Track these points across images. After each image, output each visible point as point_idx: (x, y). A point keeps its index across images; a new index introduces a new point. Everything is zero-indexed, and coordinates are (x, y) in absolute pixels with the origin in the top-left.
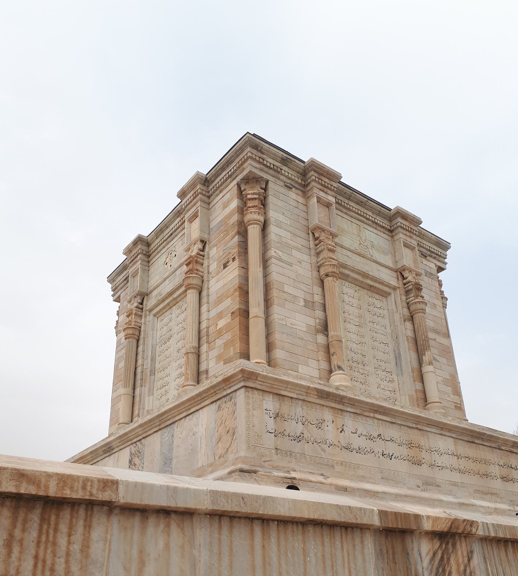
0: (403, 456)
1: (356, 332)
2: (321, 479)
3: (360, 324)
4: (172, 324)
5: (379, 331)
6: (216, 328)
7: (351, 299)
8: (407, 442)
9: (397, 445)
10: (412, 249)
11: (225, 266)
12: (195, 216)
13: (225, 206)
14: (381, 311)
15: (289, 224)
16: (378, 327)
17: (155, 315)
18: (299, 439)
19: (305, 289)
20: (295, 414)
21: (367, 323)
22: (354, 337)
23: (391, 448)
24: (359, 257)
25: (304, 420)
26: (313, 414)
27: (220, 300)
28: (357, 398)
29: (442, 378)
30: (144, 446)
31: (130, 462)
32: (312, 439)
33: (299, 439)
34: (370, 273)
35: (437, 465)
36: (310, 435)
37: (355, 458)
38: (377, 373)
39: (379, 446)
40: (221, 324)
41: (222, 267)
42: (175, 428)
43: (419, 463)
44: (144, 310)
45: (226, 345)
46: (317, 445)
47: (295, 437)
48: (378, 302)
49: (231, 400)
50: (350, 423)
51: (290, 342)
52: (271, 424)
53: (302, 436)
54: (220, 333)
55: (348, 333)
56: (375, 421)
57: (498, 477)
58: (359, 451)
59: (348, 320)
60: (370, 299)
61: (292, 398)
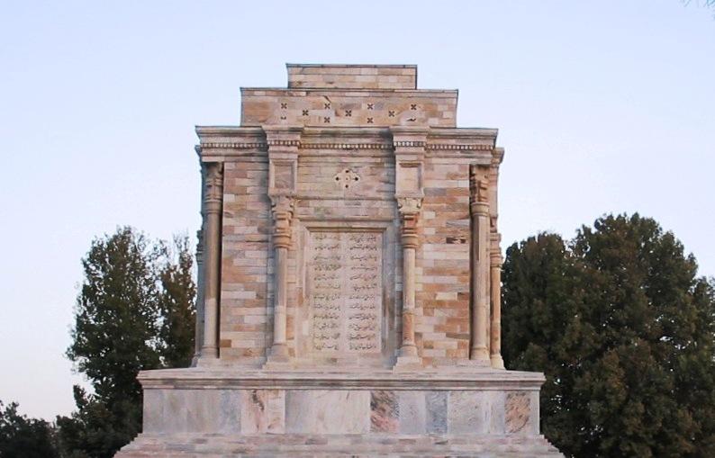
4: (340, 252)
6: (435, 297)
11: (450, 241)
12: (411, 165)
13: (453, 176)
17: (308, 228)
27: (436, 271)
30: (398, 397)
31: (374, 406)
40: (441, 296)
41: (445, 239)
42: (449, 395)
44: (295, 216)
45: (450, 320)
49: (524, 394)
54: (441, 304)
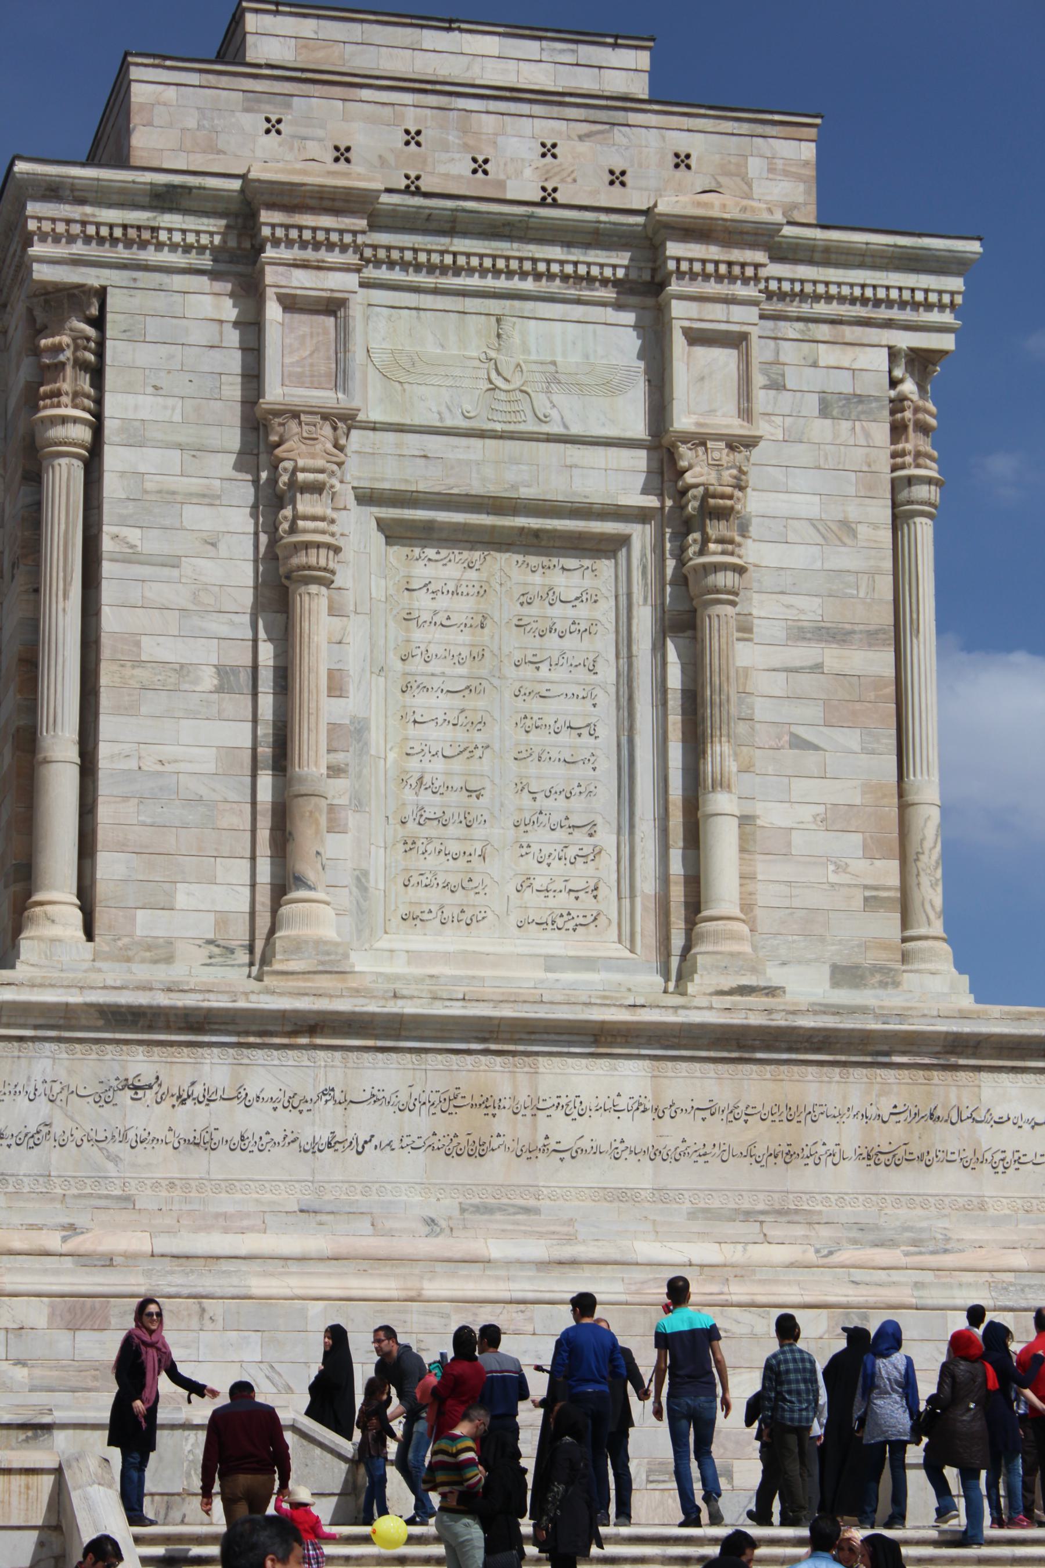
0: (414, 1137)
1: (452, 717)
2: (53, 1241)
3: (474, 683)
5: (556, 690)
7: (443, 602)
8: (434, 1098)
9: (391, 1109)
10: (736, 340)
14: (583, 611)
15: (177, 418)
16: (560, 674)
18: (32, 1140)
19: (225, 631)
20: (29, 1079)
21: (510, 671)
22: (439, 736)
24: (476, 443)
25: (57, 1088)
28: (242, 1004)
29: (821, 809)
32: (78, 1135)
33: (32, 1140)
34: (525, 492)
35: (553, 1146)
36: (71, 1124)
37: (223, 1163)
38: (525, 839)
43: (479, 1150)
46: (95, 1148)
47: (22, 1136)
48: (570, 577)
51: (149, 821)
53: (43, 1133)
55: (412, 731)
56: (321, 1054)
57: (849, 1153)
58: (241, 1144)
59: (420, 679)
60: (537, 579)
61: (21, 1039)
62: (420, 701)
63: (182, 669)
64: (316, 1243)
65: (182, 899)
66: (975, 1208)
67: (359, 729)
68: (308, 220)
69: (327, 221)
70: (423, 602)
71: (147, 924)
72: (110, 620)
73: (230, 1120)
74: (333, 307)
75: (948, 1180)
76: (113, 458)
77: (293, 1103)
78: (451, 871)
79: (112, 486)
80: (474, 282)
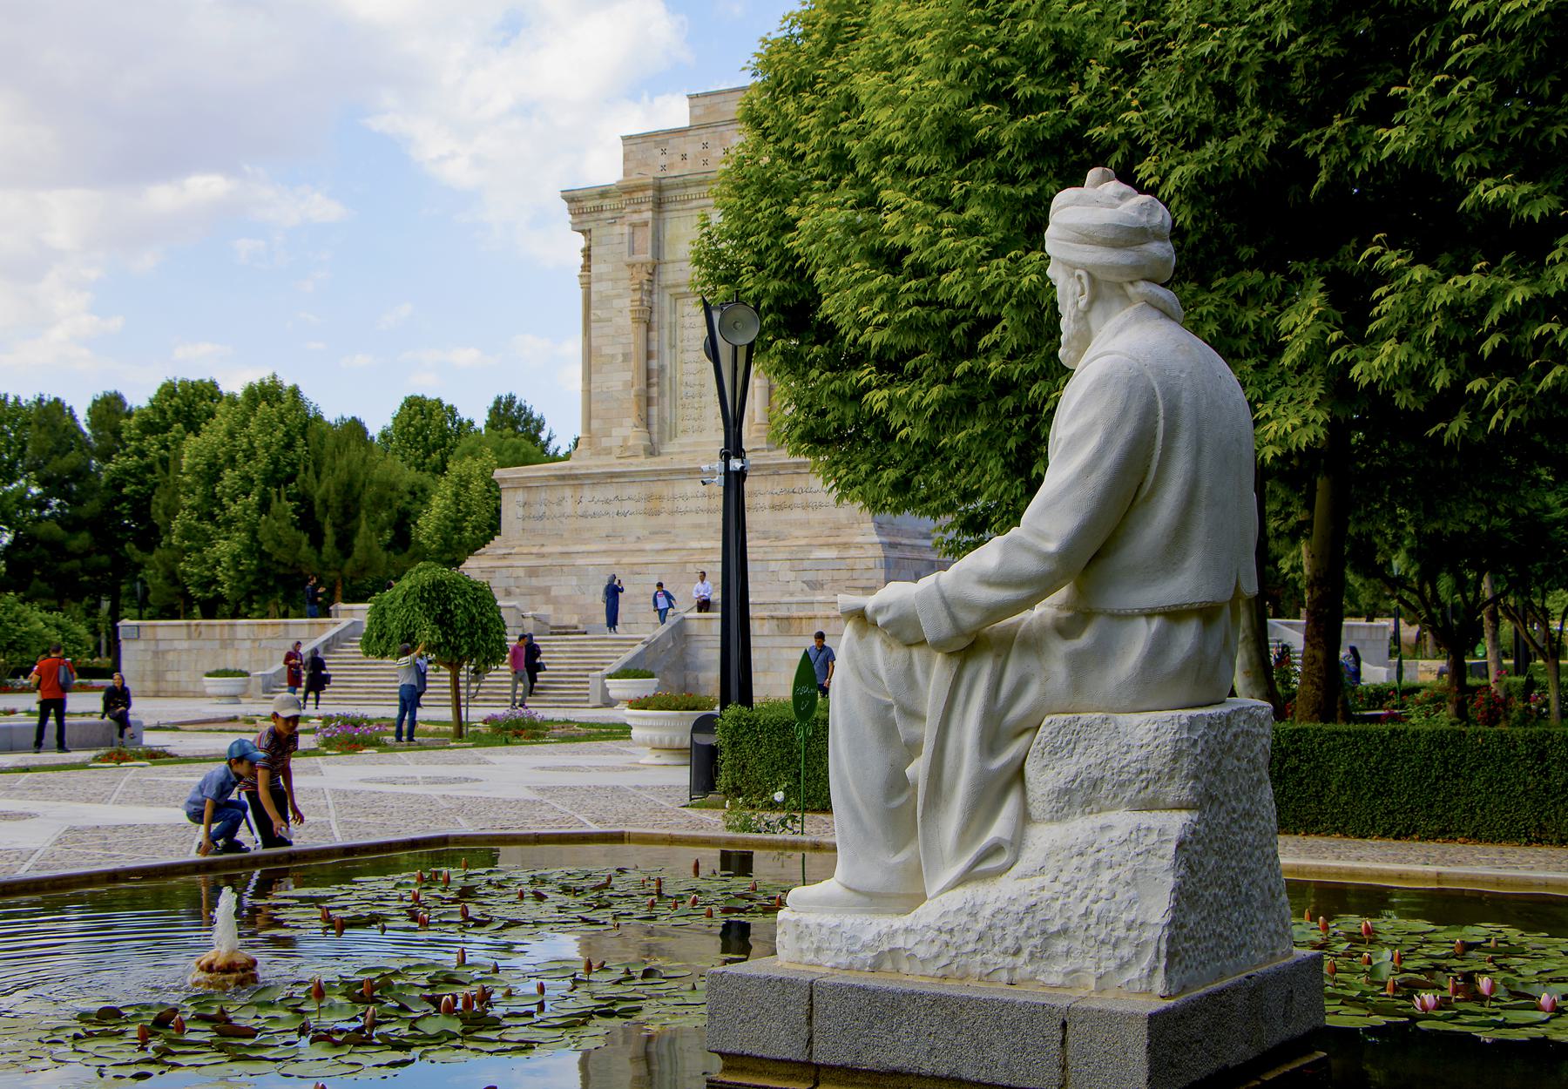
18: (541, 518)
23: (629, 506)
26: (554, 496)
33: (541, 518)
39: (613, 508)
43: (658, 513)
50: (587, 493)
52: (520, 512)
58: (594, 515)
62: (686, 356)
63: (613, 356)
64: (603, 547)
65: (616, 432)
66: (806, 524)
67: (662, 369)
68: (635, 195)
69: (640, 195)
70: (687, 321)
71: (605, 442)
72: (594, 344)
73: (593, 508)
74: (646, 224)
75: (798, 514)
76: (594, 287)
77: (607, 502)
78: (695, 413)
79: (594, 297)
80: (695, 203)
